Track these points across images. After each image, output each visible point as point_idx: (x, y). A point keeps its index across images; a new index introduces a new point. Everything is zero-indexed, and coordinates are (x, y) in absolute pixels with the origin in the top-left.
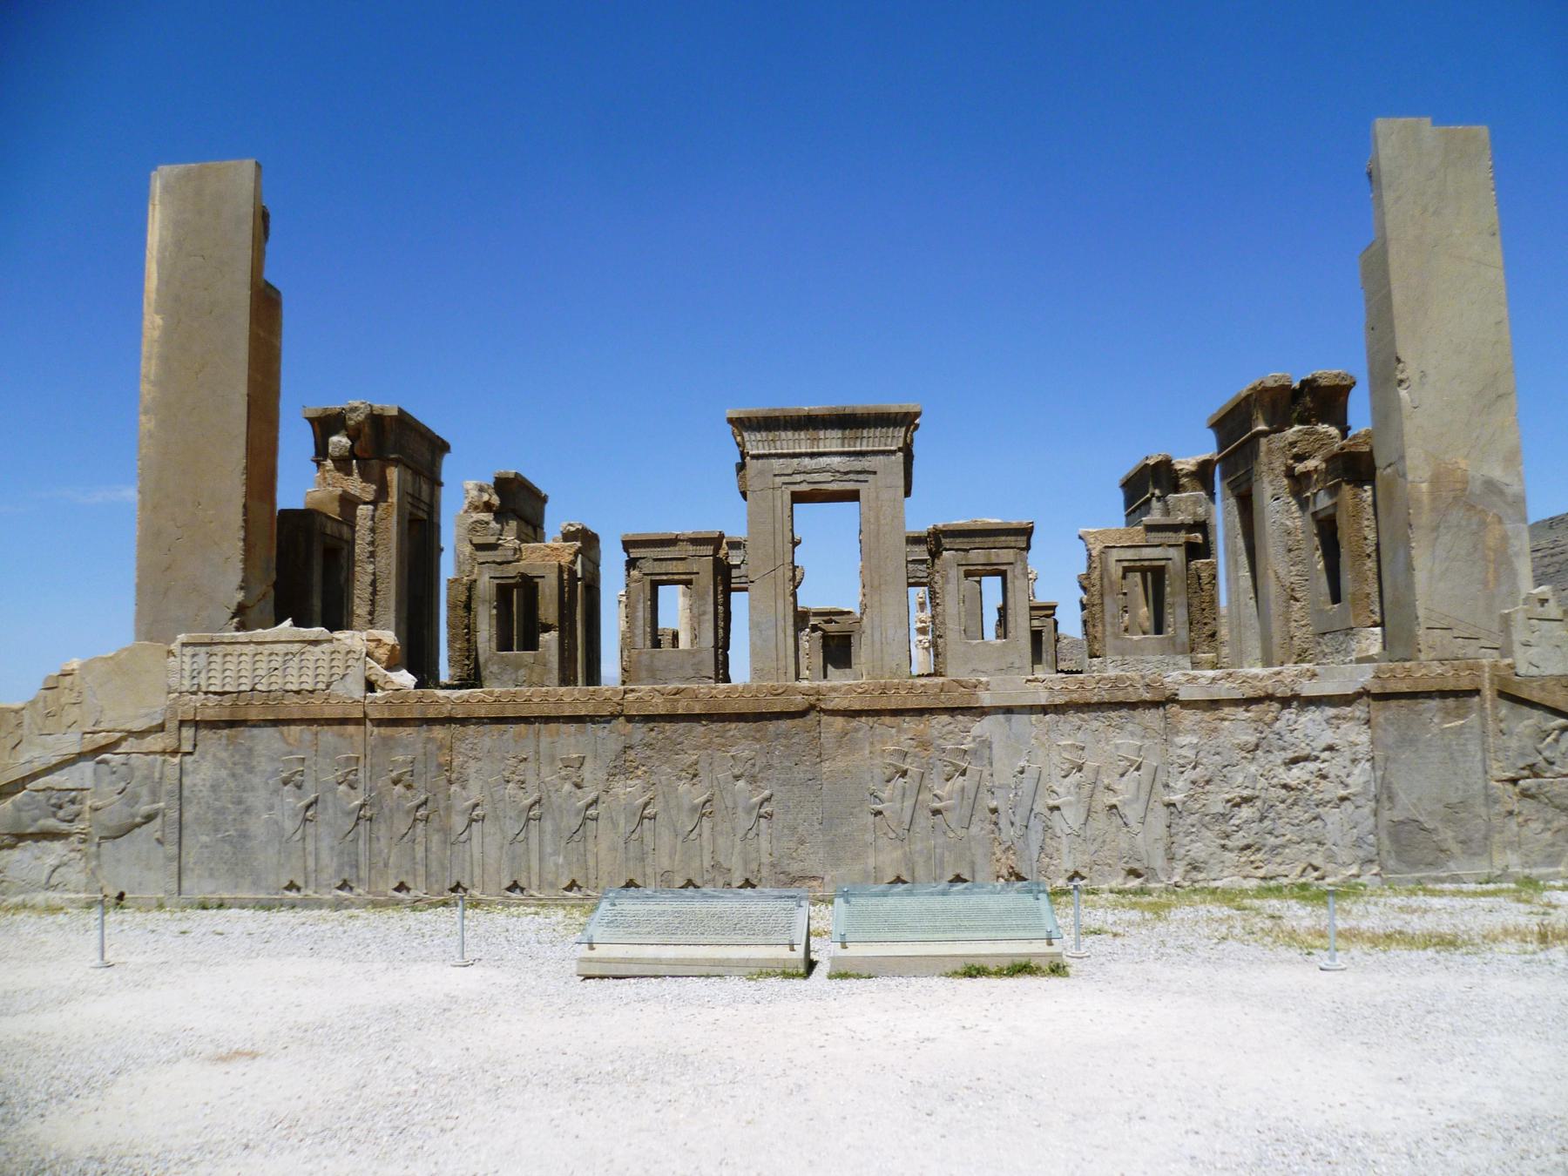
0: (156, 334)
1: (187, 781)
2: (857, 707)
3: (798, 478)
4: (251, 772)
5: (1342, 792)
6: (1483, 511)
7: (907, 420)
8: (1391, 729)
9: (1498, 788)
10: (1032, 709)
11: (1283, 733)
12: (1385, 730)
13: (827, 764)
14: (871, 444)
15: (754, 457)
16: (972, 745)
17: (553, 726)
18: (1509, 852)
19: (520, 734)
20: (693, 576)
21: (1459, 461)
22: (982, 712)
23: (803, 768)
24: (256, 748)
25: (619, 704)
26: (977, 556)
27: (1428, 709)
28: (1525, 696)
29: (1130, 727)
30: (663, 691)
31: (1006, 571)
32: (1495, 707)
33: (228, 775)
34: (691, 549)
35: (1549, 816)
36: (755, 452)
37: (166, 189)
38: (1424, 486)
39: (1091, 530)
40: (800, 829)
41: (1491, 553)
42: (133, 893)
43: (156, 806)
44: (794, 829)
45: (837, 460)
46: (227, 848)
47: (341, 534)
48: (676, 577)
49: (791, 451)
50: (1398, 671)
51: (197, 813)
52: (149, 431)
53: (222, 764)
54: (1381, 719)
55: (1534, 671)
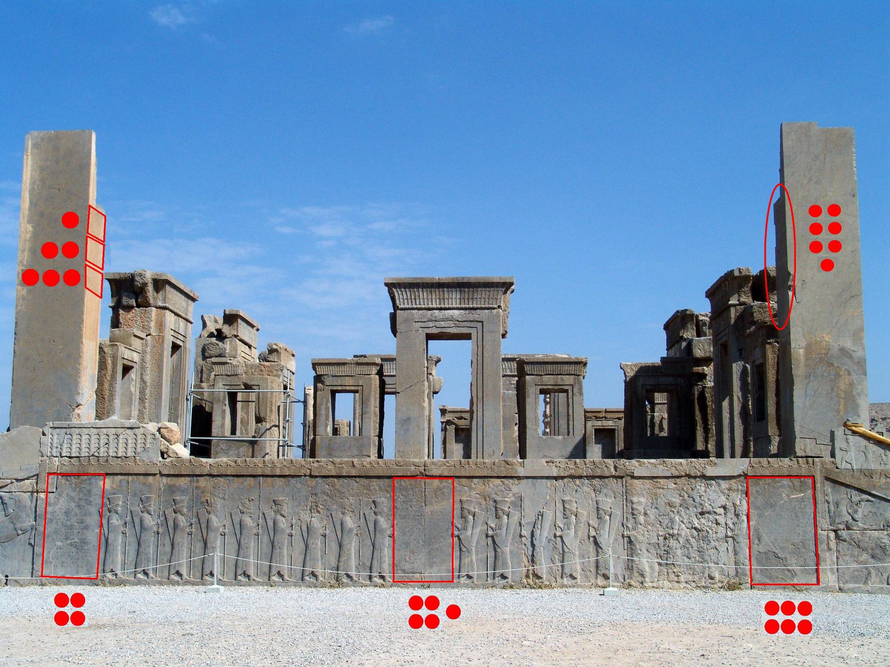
0: (28, 236)
1: (49, 509)
2: (446, 474)
3: (431, 324)
4: (90, 505)
5: (729, 534)
6: (838, 367)
7: (506, 286)
8: (760, 497)
10: (547, 478)
11: (695, 497)
12: (756, 498)
13: (428, 507)
14: (479, 303)
15: (402, 309)
16: (513, 499)
17: (269, 479)
19: (250, 485)
20: (359, 388)
21: (824, 335)
22: (519, 478)
23: (414, 508)
24: (92, 490)
25: (309, 469)
26: (549, 380)
27: (783, 486)
28: (842, 481)
29: (605, 491)
30: (334, 463)
31: (568, 390)
32: (823, 485)
33: (75, 506)
34: (359, 369)
35: (856, 554)
36: (402, 306)
37: (35, 145)
38: (801, 351)
39: (628, 363)
40: (412, 544)
42: (12, 576)
43: (30, 524)
44: (407, 544)
45: (456, 312)
46: (74, 550)
47: (132, 358)
48: (348, 388)
49: (427, 306)
50: (765, 463)
51: (56, 528)
52: (23, 295)
53: (72, 499)
54: (754, 492)
55: (849, 466)
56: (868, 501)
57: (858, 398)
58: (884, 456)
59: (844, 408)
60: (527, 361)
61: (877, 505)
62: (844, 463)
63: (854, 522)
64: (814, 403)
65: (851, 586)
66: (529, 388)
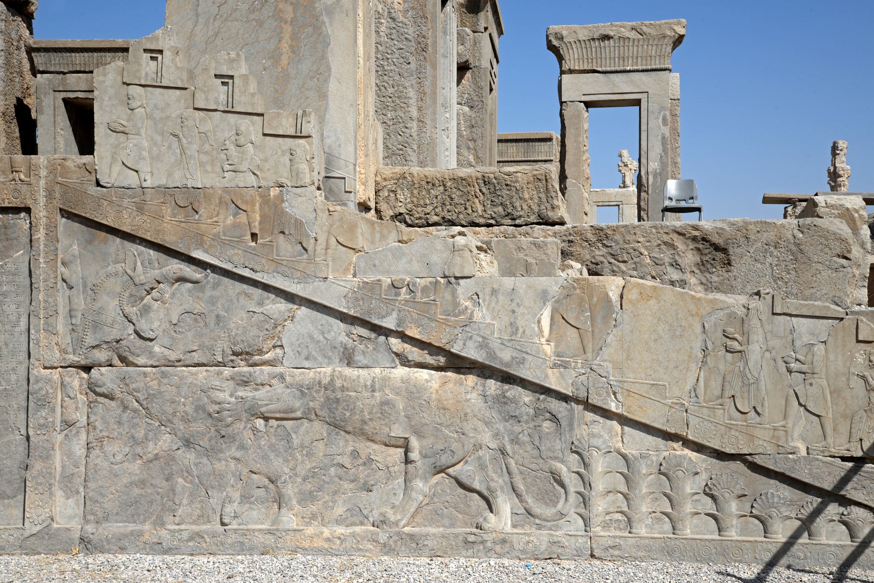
9: (49, 381)
18: (59, 494)
28: (109, 222)
32: (52, 237)
35: (140, 434)
41: (290, 9)
55: (132, 180)
56: (182, 280)
57: (326, 20)
58: (232, 148)
59: (291, 47)
60: (35, 46)
61: (209, 293)
62: (118, 167)
63: (140, 342)
64: (216, 35)
65: (115, 528)
66: (42, 96)
